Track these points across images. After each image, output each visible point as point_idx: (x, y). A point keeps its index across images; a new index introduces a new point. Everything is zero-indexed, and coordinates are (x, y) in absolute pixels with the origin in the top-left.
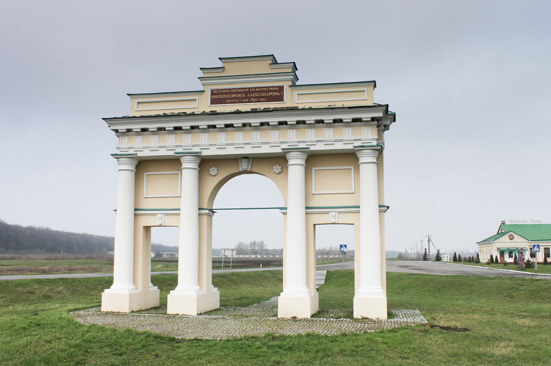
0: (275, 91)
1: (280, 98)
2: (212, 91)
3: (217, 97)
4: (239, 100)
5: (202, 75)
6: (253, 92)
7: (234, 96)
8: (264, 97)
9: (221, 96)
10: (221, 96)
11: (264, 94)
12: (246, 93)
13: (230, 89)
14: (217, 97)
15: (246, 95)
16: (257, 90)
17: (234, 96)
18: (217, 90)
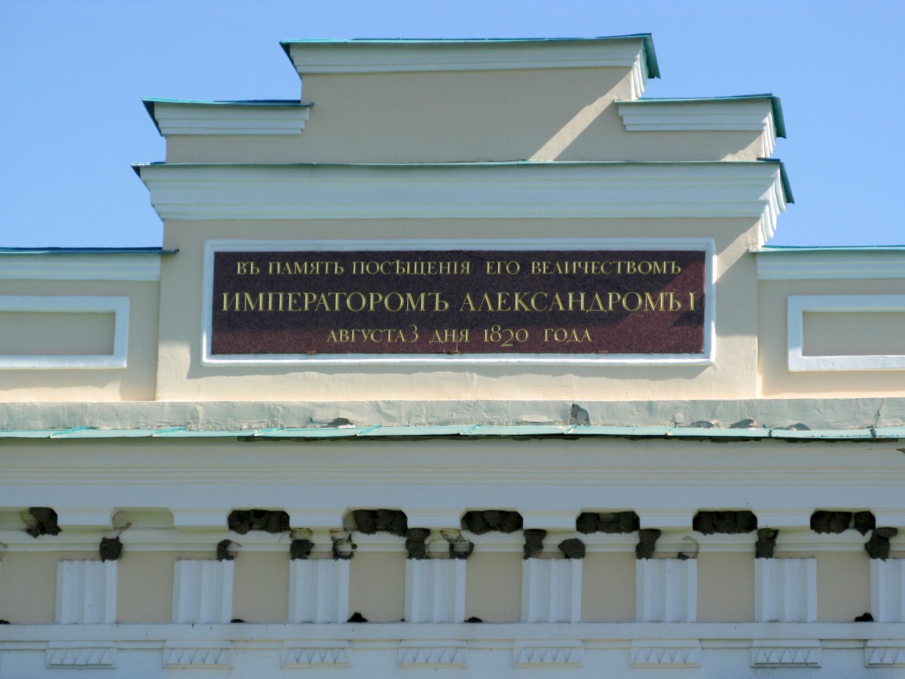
0: (656, 283)
1: (683, 333)
2: (225, 262)
3: (264, 302)
4: (409, 336)
5: (155, 149)
6: (493, 285)
7: (369, 302)
8: (575, 319)
9: (287, 302)
10: (287, 302)
11: (573, 301)
12: (453, 288)
13: (345, 258)
14: (264, 302)
15: (456, 299)
16: (539, 268)
17: (369, 302)
18: (262, 258)
